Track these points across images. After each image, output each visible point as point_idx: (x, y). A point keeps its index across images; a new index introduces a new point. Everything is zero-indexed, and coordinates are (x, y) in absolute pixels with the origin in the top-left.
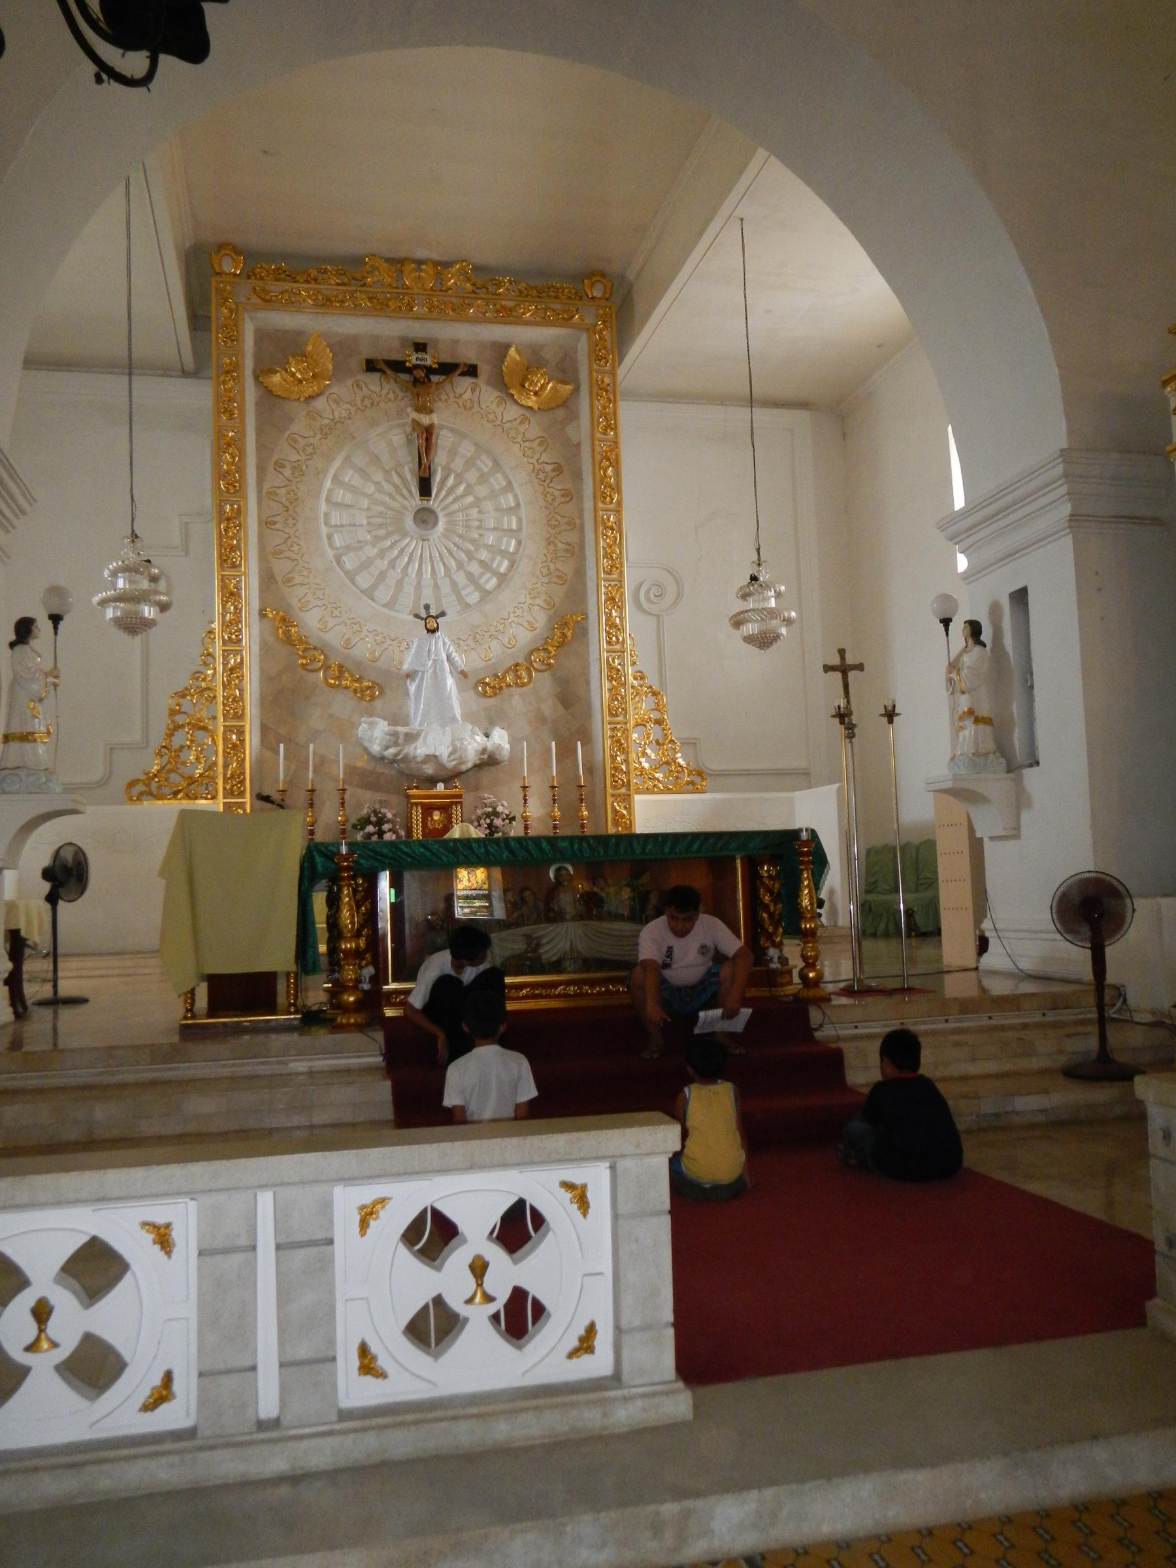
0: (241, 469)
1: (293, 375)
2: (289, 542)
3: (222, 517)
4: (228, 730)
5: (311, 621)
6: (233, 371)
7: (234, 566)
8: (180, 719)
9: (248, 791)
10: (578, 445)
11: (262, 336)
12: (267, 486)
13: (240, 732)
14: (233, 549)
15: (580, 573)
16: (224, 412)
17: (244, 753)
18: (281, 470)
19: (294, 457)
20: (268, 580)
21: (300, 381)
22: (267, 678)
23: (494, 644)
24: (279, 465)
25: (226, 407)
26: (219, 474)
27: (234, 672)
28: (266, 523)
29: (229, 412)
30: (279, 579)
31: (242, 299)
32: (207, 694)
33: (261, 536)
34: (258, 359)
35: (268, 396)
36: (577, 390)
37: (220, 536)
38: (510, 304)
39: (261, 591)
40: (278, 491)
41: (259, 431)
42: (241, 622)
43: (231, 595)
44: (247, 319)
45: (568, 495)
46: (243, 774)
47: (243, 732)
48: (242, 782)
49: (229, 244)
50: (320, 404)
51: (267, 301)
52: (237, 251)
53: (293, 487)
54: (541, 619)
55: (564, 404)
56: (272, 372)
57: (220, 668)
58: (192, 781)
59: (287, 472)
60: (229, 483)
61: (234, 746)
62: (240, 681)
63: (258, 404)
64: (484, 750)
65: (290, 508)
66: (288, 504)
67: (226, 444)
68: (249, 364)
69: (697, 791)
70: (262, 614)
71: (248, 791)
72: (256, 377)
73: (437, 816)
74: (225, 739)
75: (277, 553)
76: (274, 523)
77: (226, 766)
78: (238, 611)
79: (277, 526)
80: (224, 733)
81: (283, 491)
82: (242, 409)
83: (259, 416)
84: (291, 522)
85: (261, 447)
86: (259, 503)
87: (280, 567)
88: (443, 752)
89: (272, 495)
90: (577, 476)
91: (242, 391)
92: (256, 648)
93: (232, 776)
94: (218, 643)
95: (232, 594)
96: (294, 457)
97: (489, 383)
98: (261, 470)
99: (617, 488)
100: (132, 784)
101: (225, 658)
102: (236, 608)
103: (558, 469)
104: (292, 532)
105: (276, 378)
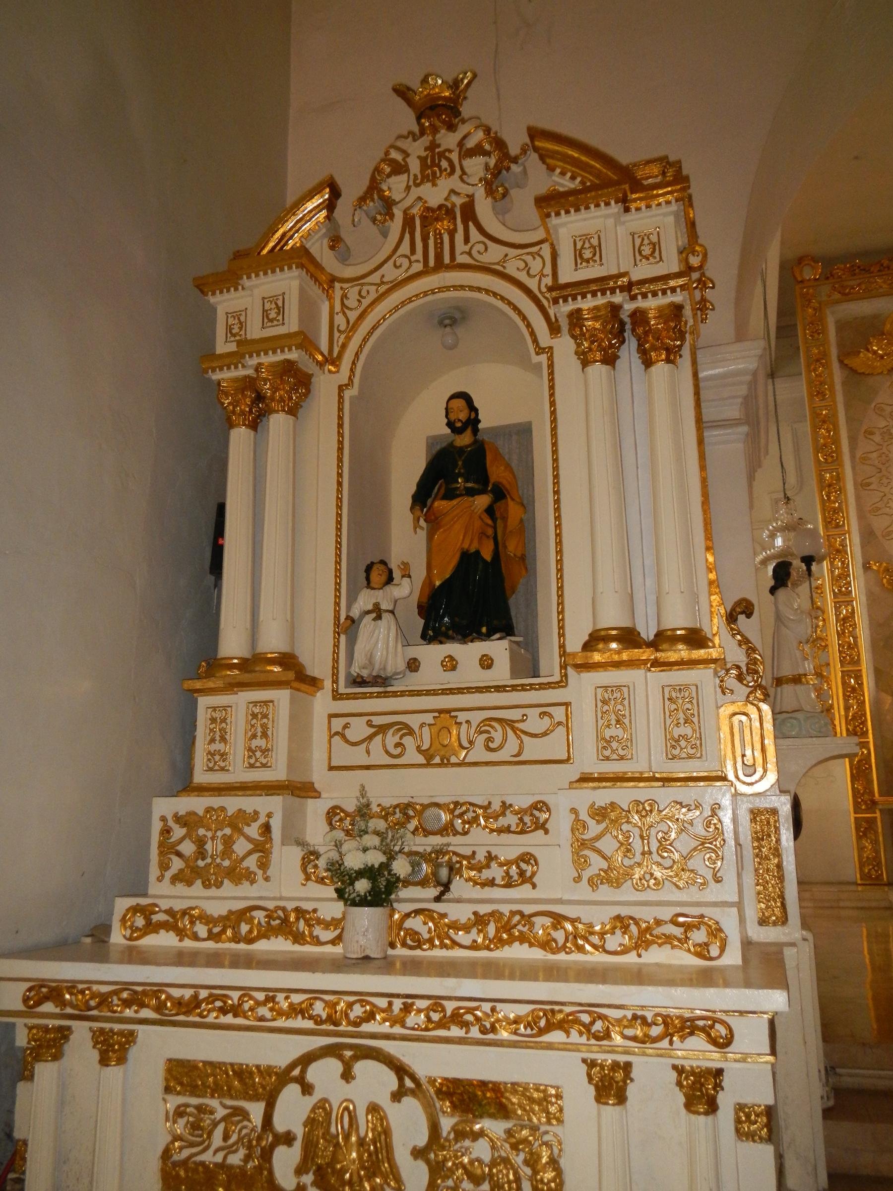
0: (836, 441)
1: (875, 352)
2: (885, 499)
3: (822, 484)
6: (821, 359)
7: (837, 526)
9: (870, 731)
11: (841, 326)
12: (859, 454)
13: (858, 677)
14: (836, 511)
16: (816, 395)
17: (863, 696)
18: (871, 437)
19: (882, 423)
21: (882, 357)
22: (875, 626)
24: (869, 433)
25: (818, 391)
27: (847, 621)
28: (862, 486)
29: (821, 394)
30: (878, 533)
31: (825, 298)
33: (858, 498)
34: (840, 345)
35: (854, 375)
37: (823, 502)
39: (863, 547)
40: (870, 455)
41: (848, 406)
42: (849, 575)
44: (828, 312)
46: (865, 715)
47: (861, 676)
48: (864, 723)
49: (807, 256)
51: (847, 296)
52: (815, 260)
53: (884, 450)
57: (833, 618)
59: (877, 438)
60: (827, 453)
61: (854, 690)
62: (854, 629)
63: (844, 384)
65: (883, 469)
66: (880, 466)
67: (822, 421)
68: (834, 352)
70: (866, 567)
71: (870, 731)
72: (841, 362)
74: (844, 683)
75: (875, 510)
76: (869, 484)
77: (847, 709)
78: (845, 566)
79: (871, 487)
80: (843, 677)
81: (875, 455)
82: (832, 389)
83: (846, 394)
84: (885, 481)
85: (849, 420)
86: (853, 468)
87: (879, 524)
89: (864, 459)
91: (831, 375)
92: (864, 598)
93: (854, 717)
94: (829, 597)
95: (838, 551)
96: (882, 423)
98: (853, 440)
101: (837, 609)
102: (843, 563)
104: (887, 490)
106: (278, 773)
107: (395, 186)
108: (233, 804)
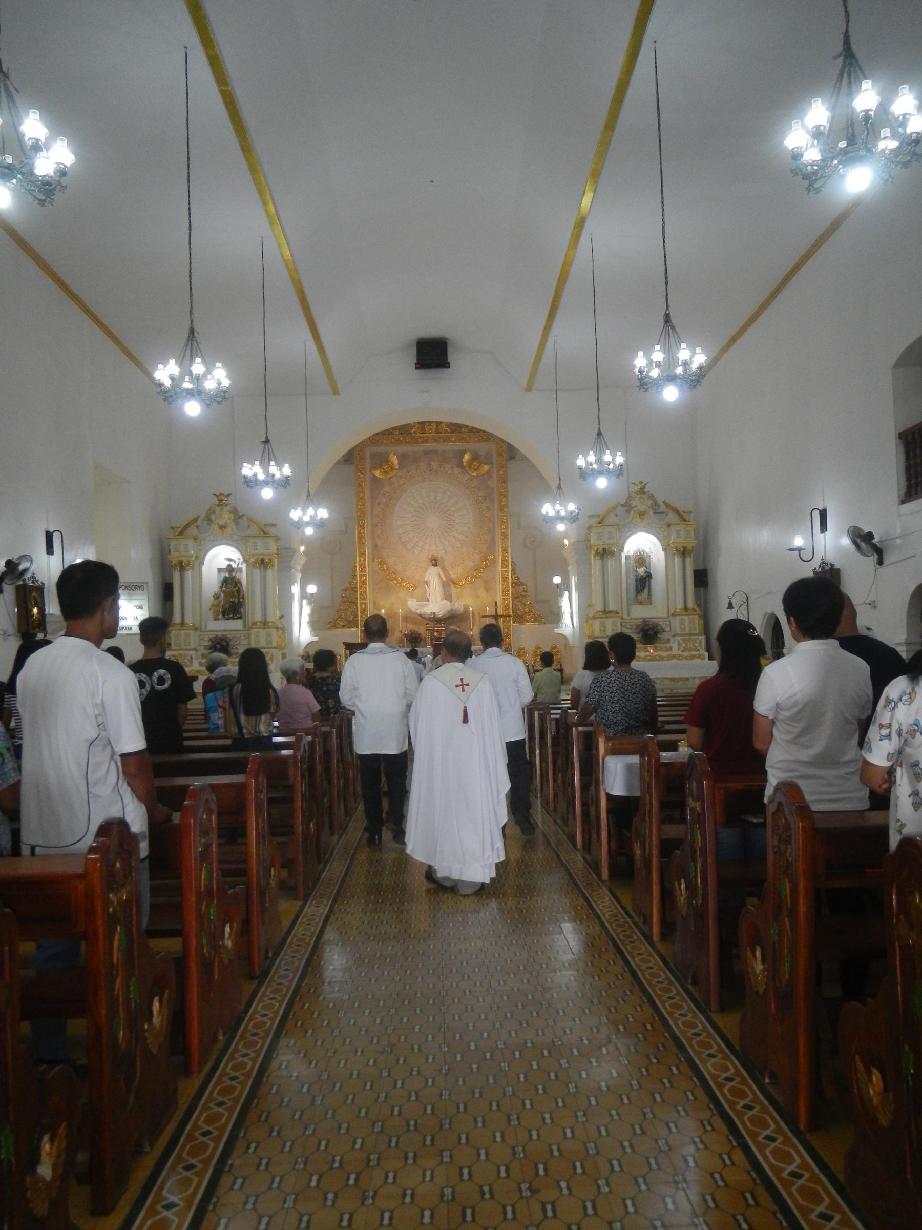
4: (361, 603)
5: (391, 561)
6: (362, 471)
8: (345, 599)
10: (492, 489)
11: (373, 456)
13: (366, 604)
15: (493, 538)
19: (384, 500)
20: (375, 547)
23: (459, 568)
24: (379, 504)
26: (358, 510)
27: (363, 582)
28: (375, 526)
29: (360, 485)
32: (354, 589)
36: (492, 467)
38: (465, 435)
43: (362, 554)
45: (488, 509)
50: (394, 480)
54: (477, 557)
55: (487, 473)
56: (376, 468)
58: (349, 622)
60: (362, 514)
64: (452, 610)
67: (361, 499)
68: (368, 467)
69: (541, 623)
70: (373, 560)
73: (436, 634)
88: (436, 611)
90: (492, 500)
96: (384, 500)
97: (458, 466)
99: (506, 506)
100: (329, 623)
103: (485, 498)
105: (377, 473)
106: (192, 646)
107: (213, 517)
108: (184, 653)
